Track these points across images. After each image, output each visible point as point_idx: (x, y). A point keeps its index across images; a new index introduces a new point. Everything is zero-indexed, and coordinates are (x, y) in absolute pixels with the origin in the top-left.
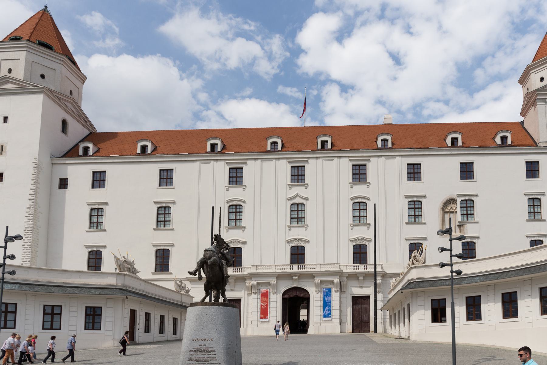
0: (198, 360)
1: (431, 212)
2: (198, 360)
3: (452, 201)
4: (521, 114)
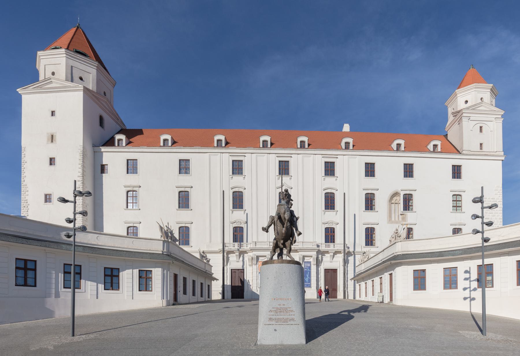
0: (277, 320)
1: (381, 202)
2: (277, 320)
3: (396, 194)
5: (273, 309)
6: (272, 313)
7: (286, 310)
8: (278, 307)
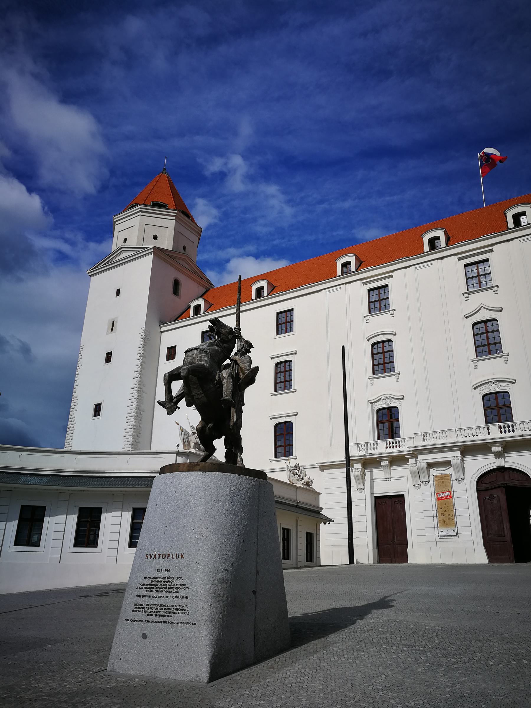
0: (153, 610)
6: (143, 592)
8: (157, 575)
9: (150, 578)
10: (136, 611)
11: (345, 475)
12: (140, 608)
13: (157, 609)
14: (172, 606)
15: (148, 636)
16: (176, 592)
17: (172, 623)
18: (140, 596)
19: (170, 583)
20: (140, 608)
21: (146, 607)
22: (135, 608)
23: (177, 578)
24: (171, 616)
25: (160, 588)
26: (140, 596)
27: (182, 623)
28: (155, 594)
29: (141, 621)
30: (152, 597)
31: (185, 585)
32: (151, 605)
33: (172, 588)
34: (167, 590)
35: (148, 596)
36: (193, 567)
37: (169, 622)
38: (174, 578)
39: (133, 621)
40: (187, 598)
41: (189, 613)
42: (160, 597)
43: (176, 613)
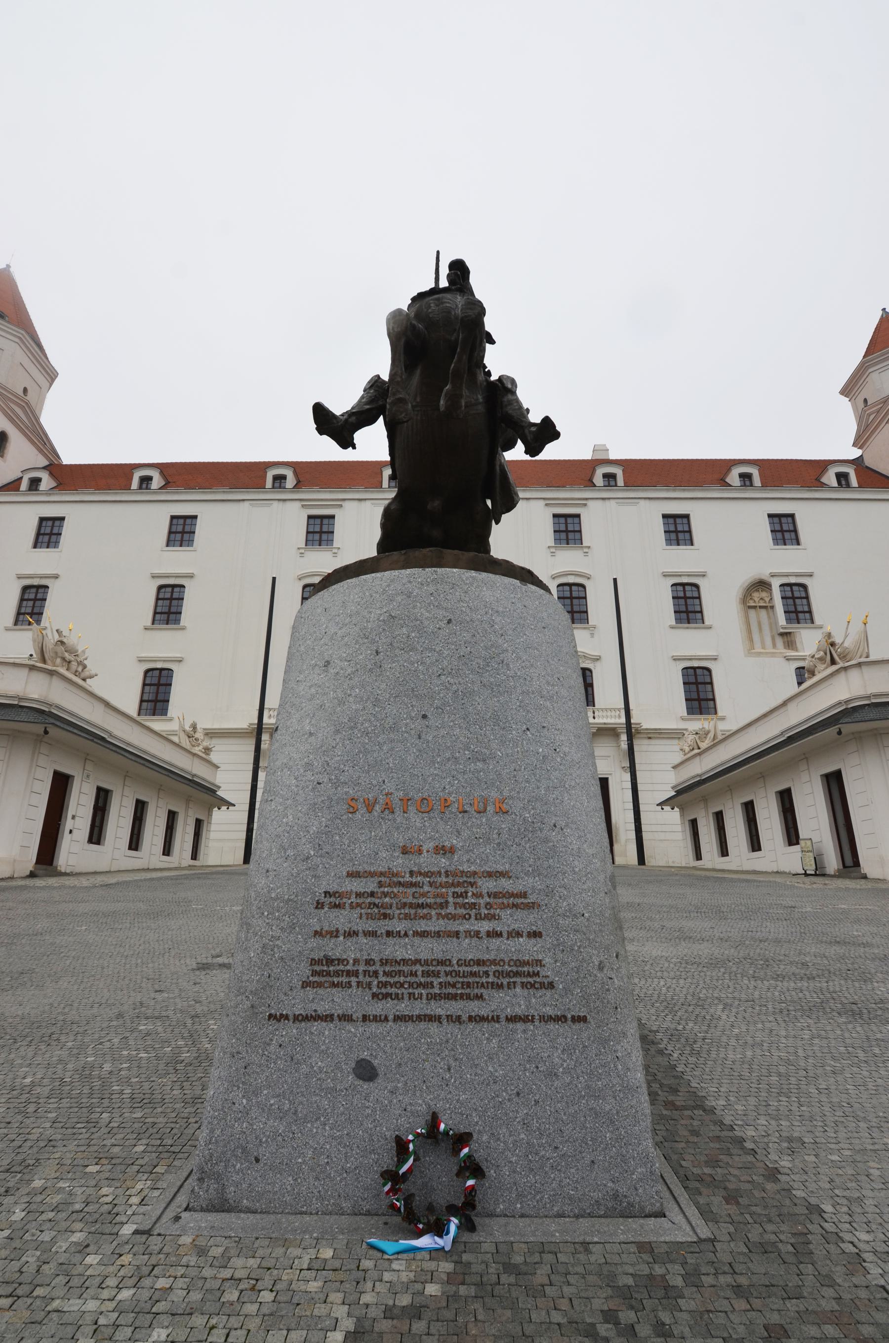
0: (389, 980)
2: (389, 980)
4: (854, 445)
5: (357, 885)
6: (342, 919)
7: (456, 894)
8: (400, 863)
9: (372, 874)
10: (320, 985)
11: (253, 748)
12: (337, 973)
13: (415, 974)
14: (479, 962)
15: (381, 1071)
16: (491, 917)
17: (483, 1019)
18: (334, 934)
19: (459, 890)
20: (337, 973)
21: (361, 968)
22: (315, 973)
23: (490, 875)
24: (480, 997)
25: (422, 906)
26: (334, 934)
27: (526, 1019)
28: (400, 926)
29: (346, 1018)
30: (389, 934)
31: (524, 895)
32: (384, 962)
33: (473, 906)
34: (451, 909)
35: (373, 934)
36: (546, 840)
37: (471, 1019)
38: (475, 873)
39: (307, 1018)
40: (536, 935)
41: (551, 985)
42: (423, 934)
43: (500, 987)
